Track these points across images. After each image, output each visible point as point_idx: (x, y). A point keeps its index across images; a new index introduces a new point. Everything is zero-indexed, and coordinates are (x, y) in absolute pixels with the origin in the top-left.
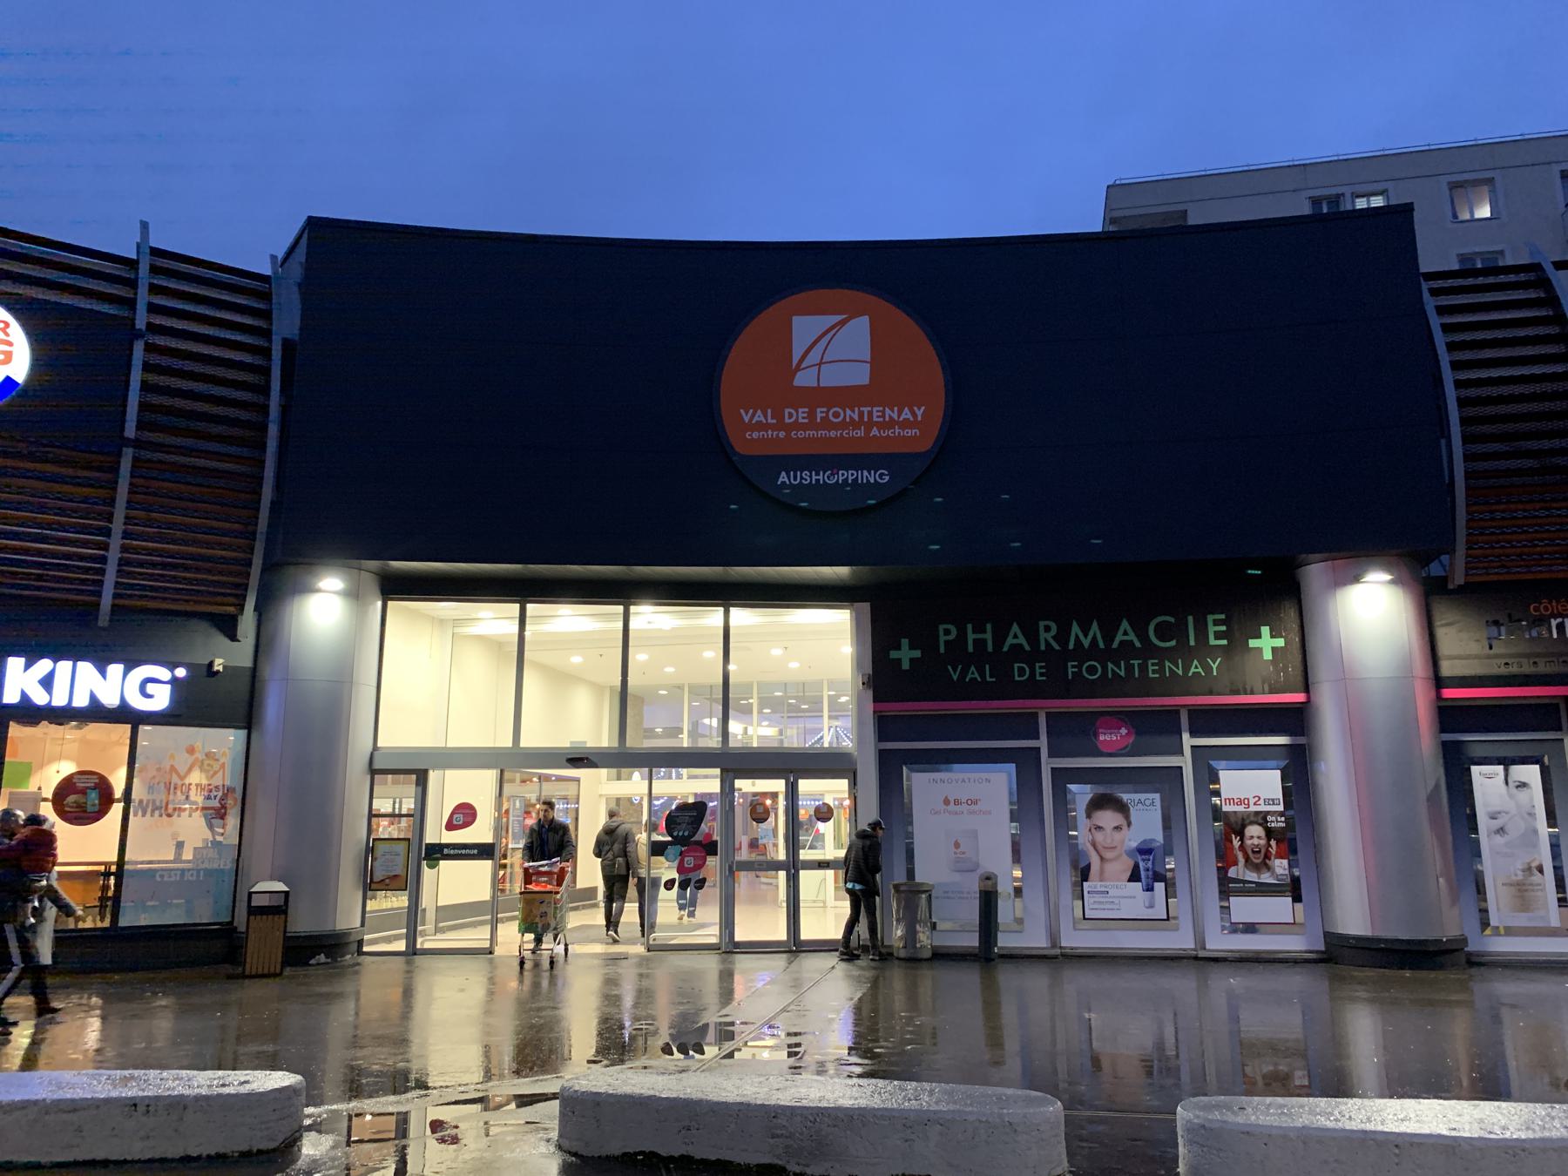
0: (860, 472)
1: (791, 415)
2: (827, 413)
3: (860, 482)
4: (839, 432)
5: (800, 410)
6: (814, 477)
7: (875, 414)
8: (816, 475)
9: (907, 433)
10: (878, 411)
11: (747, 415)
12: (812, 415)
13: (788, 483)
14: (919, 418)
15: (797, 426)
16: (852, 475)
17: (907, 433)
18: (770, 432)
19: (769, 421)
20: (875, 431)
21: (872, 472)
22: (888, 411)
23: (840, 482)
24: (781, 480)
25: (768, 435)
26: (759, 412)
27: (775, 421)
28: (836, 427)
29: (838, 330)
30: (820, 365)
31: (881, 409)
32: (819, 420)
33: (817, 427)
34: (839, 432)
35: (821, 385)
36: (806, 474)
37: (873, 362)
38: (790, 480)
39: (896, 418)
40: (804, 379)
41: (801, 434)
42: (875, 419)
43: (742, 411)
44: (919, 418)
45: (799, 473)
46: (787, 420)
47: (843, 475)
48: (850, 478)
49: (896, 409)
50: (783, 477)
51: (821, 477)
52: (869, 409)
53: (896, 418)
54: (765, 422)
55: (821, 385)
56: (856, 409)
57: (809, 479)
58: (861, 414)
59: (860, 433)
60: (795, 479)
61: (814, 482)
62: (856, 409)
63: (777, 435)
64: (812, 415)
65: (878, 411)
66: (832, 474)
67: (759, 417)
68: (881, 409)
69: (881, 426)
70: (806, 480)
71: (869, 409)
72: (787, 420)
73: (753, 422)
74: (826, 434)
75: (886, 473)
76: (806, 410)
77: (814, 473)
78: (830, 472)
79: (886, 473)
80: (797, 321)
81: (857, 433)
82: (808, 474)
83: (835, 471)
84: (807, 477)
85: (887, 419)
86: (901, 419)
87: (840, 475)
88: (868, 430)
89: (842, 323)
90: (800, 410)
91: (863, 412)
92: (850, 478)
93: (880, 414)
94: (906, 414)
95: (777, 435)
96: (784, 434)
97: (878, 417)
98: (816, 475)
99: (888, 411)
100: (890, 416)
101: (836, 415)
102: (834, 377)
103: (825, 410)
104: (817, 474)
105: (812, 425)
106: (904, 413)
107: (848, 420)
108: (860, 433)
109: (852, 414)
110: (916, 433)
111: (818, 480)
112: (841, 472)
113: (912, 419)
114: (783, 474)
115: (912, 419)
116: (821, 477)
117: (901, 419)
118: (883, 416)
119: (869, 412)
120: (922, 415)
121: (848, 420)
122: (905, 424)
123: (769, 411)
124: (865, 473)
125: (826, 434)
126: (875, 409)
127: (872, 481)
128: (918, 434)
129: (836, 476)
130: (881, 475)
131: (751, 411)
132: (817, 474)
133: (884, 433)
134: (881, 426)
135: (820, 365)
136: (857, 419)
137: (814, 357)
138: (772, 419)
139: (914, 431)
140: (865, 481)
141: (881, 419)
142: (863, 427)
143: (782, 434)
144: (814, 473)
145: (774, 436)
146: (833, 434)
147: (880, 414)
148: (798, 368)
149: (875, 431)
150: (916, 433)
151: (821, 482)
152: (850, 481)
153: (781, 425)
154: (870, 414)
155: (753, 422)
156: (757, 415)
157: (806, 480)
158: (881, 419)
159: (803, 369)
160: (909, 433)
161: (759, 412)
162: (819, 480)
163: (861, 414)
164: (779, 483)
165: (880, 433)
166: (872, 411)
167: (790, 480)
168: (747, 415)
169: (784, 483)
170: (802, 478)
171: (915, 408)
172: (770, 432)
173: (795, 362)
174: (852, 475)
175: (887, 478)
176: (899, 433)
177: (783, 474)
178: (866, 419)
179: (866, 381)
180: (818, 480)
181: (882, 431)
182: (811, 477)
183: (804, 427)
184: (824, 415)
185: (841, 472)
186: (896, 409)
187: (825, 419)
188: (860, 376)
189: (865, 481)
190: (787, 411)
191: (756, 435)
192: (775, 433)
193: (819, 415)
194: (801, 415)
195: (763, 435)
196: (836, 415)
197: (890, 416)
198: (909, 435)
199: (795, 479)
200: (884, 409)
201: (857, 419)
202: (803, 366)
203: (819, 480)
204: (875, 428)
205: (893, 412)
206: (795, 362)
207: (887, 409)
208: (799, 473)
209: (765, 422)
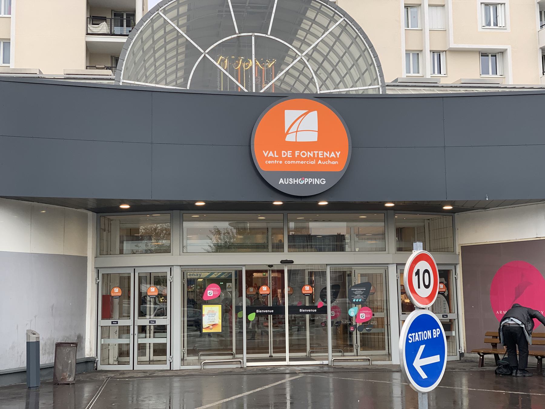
0: (313, 179)
1: (284, 154)
2: (300, 153)
3: (313, 183)
4: (305, 162)
5: (289, 152)
6: (294, 181)
7: (320, 154)
8: (295, 180)
9: (333, 163)
10: (321, 153)
11: (266, 153)
12: (293, 154)
13: (283, 183)
14: (338, 157)
15: (287, 158)
16: (310, 180)
17: (333, 163)
18: (276, 161)
19: (276, 156)
21: (319, 179)
23: (305, 183)
25: (275, 162)
26: (271, 152)
27: (278, 156)
28: (304, 159)
30: (297, 131)
31: (322, 152)
32: (296, 156)
33: (296, 159)
34: (305, 162)
35: (297, 141)
36: (291, 180)
38: (284, 182)
39: (328, 155)
40: (290, 138)
41: (289, 162)
42: (320, 157)
43: (264, 151)
44: (338, 157)
45: (288, 179)
46: (283, 156)
47: (306, 180)
48: (310, 182)
49: (328, 152)
50: (281, 181)
51: (297, 181)
52: (317, 152)
54: (273, 156)
55: (297, 141)
56: (312, 152)
57: (292, 182)
59: (313, 162)
60: (286, 182)
61: (294, 183)
62: (312, 152)
65: (321, 153)
66: (302, 180)
67: (271, 154)
68: (322, 152)
70: (291, 182)
71: (317, 152)
72: (283, 156)
73: (269, 156)
74: (299, 162)
76: (291, 152)
77: (294, 179)
78: (301, 179)
79: (325, 180)
80: (287, 113)
82: (292, 180)
84: (292, 181)
85: (325, 157)
87: (305, 180)
88: (317, 162)
89: (306, 114)
91: (315, 153)
92: (310, 182)
93: (322, 154)
95: (279, 162)
96: (282, 162)
97: (321, 155)
98: (295, 180)
99: (325, 153)
100: (326, 156)
101: (304, 154)
102: (303, 138)
103: (299, 152)
104: (296, 180)
105: (293, 158)
106: (332, 154)
107: (308, 156)
108: (313, 162)
110: (337, 163)
111: (296, 183)
112: (305, 179)
113: (335, 157)
114: (281, 179)
115: (335, 157)
116: (297, 181)
117: (331, 157)
118: (323, 155)
119: (317, 153)
120: (339, 155)
121: (308, 156)
122: (332, 159)
123: (275, 152)
124: (316, 179)
125: (299, 162)
126: (320, 152)
127: (319, 183)
128: (338, 163)
129: (304, 181)
130: (322, 181)
131: (268, 152)
132: (296, 180)
134: (323, 159)
135: (297, 131)
136: (312, 156)
137: (294, 129)
138: (276, 155)
139: (336, 162)
140: (316, 183)
141: (322, 157)
142: (315, 160)
143: (281, 162)
144: (294, 179)
145: (278, 163)
146: (302, 162)
147: (322, 154)
148: (287, 133)
149: (320, 162)
151: (297, 183)
152: (309, 183)
153: (280, 158)
154: (318, 154)
155: (269, 156)
156: (270, 154)
157: (291, 182)
158: (322, 157)
159: (290, 133)
160: (334, 163)
161: (271, 152)
162: (296, 182)
163: (314, 154)
164: (280, 183)
165: (322, 163)
166: (319, 153)
167: (284, 182)
168: (266, 153)
170: (289, 181)
171: (336, 152)
172: (276, 161)
173: (286, 131)
174: (310, 180)
175: (325, 182)
176: (330, 163)
177: (281, 179)
178: (316, 157)
179: (316, 139)
180: (296, 183)
181: (323, 162)
182: (293, 181)
184: (298, 154)
185: (305, 179)
186: (328, 152)
187: (299, 156)
188: (313, 137)
189: (316, 183)
190: (283, 152)
191: (269, 162)
192: (278, 162)
193: (296, 154)
194: (289, 154)
195: (273, 162)
196: (304, 154)
197: (326, 156)
198: (334, 163)
199: (286, 182)
200: (324, 152)
201: (312, 156)
202: (289, 133)
203: (296, 182)
204: (320, 161)
205: (327, 154)
206: (286, 131)
207: (325, 152)
208: (288, 179)
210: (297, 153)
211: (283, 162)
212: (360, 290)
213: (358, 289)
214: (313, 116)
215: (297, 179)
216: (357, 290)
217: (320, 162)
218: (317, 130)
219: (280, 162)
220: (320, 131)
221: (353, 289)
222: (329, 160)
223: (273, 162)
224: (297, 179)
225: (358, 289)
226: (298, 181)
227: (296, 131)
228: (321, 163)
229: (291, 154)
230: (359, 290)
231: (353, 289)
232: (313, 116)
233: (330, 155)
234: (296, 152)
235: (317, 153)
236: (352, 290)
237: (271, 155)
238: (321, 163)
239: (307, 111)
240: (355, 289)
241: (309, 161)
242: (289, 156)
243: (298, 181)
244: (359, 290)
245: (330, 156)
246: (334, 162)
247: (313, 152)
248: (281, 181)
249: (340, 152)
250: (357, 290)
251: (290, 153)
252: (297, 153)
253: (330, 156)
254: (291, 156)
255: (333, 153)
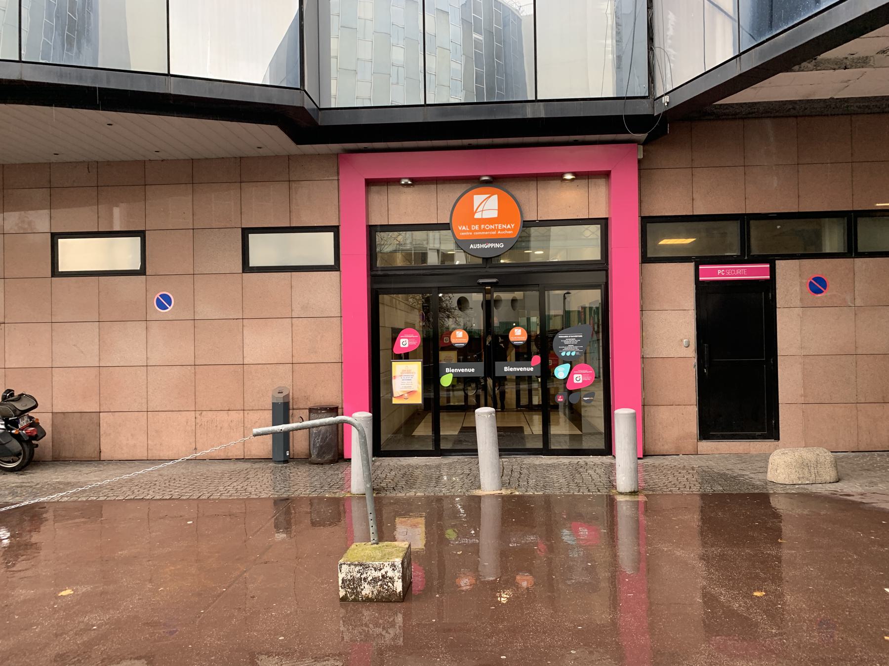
5: (477, 226)
6: (481, 246)
7: (499, 227)
12: (480, 227)
15: (475, 231)
19: (467, 229)
20: (499, 232)
26: (464, 227)
30: (482, 211)
37: (499, 210)
39: (505, 227)
40: (477, 216)
41: (477, 233)
42: (499, 228)
50: (472, 246)
58: (495, 226)
59: (494, 233)
67: (464, 228)
69: (501, 230)
72: (473, 229)
84: (479, 246)
88: (497, 232)
89: (489, 197)
99: (503, 226)
101: (487, 227)
102: (487, 215)
105: (480, 230)
108: (494, 233)
114: (472, 245)
116: (483, 246)
122: (508, 230)
126: (499, 225)
127: (498, 247)
134: (501, 230)
135: (482, 211)
137: (480, 209)
143: (471, 234)
146: (486, 233)
148: (476, 212)
153: (470, 231)
154: (498, 227)
160: (510, 232)
161: (464, 227)
163: (495, 226)
173: (475, 210)
177: (472, 245)
179: (496, 216)
187: (484, 228)
188: (494, 214)
190: (472, 226)
191: (463, 234)
196: (487, 227)
206: (475, 210)
210: (482, 226)
211: (473, 234)
212: (572, 338)
213: (570, 336)
214: (495, 198)
216: (568, 338)
217: (499, 232)
220: (499, 210)
221: (562, 337)
225: (570, 336)
226: (483, 246)
230: (571, 338)
231: (562, 337)
232: (495, 198)
233: (507, 227)
236: (559, 337)
240: (565, 337)
243: (483, 246)
244: (571, 338)
250: (568, 338)
253: (507, 227)
255: (509, 225)
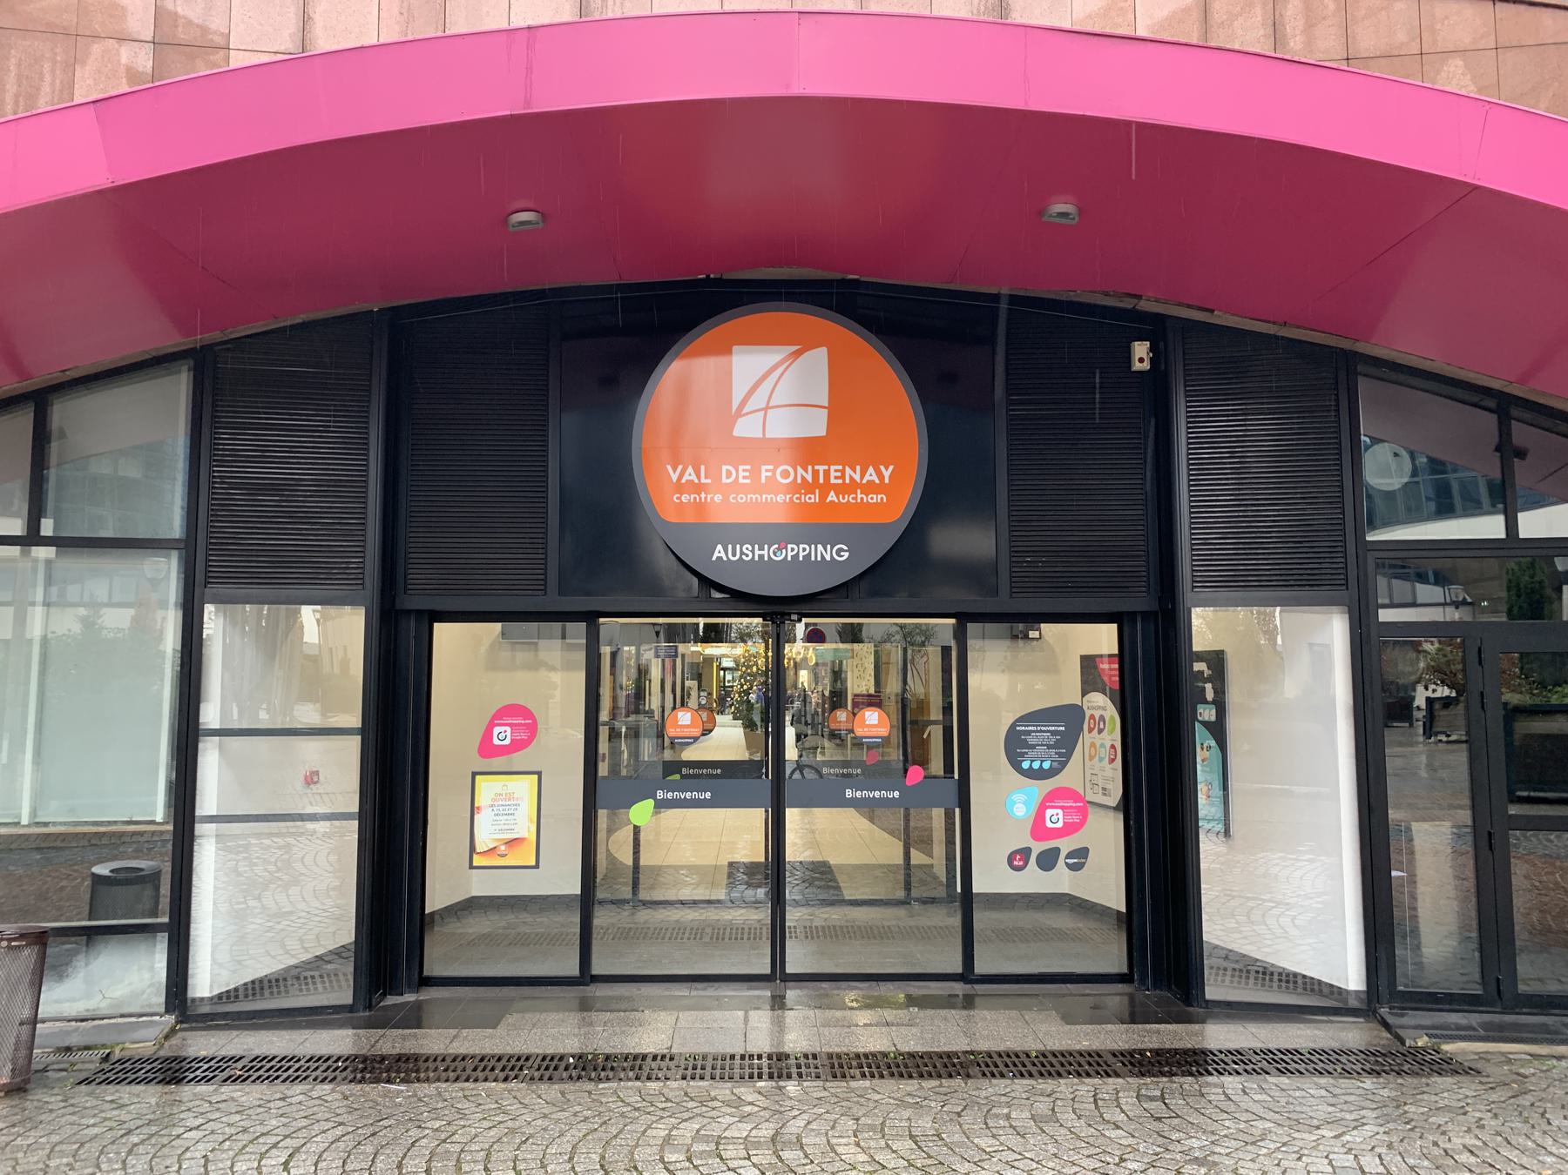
0: (813, 546)
1: (729, 474)
2: (774, 471)
3: (813, 559)
4: (788, 497)
5: (741, 468)
6: (757, 552)
7: (833, 474)
10: (836, 471)
11: (674, 472)
12: (755, 474)
13: (725, 559)
14: (887, 481)
15: (736, 487)
16: (804, 550)
18: (703, 495)
19: (703, 480)
21: (829, 546)
22: (848, 471)
23: (789, 559)
24: (716, 555)
25: (700, 499)
26: (690, 470)
29: (788, 367)
30: (766, 409)
31: (840, 467)
32: (763, 480)
39: (858, 481)
41: (742, 498)
42: (833, 481)
43: (669, 467)
44: (887, 481)
45: (738, 546)
46: (725, 480)
47: (793, 550)
48: (802, 554)
49: (858, 468)
50: (719, 552)
51: (765, 553)
52: (826, 467)
53: (858, 481)
54: (696, 481)
55: (767, 436)
56: (810, 468)
59: (813, 498)
60: (734, 555)
61: (756, 559)
62: (810, 468)
63: (712, 498)
64: (755, 474)
65: (836, 471)
66: (778, 549)
69: (840, 490)
70: (747, 556)
71: (826, 467)
72: (725, 480)
73: (683, 481)
75: (846, 548)
76: (748, 467)
77: (756, 546)
78: (776, 546)
79: (846, 548)
81: (810, 498)
82: (750, 548)
83: (783, 544)
84: (749, 552)
85: (847, 481)
86: (864, 481)
88: (824, 496)
90: (741, 468)
92: (802, 554)
93: (839, 474)
94: (871, 475)
95: (712, 498)
96: (721, 497)
97: (836, 478)
99: (848, 471)
103: (771, 467)
104: (761, 549)
105: (756, 487)
106: (868, 473)
109: (804, 474)
110: (882, 498)
111: (761, 557)
112: (790, 546)
113: (877, 481)
114: (719, 547)
115: (877, 481)
116: (765, 553)
117: (864, 481)
118: (843, 477)
119: (824, 471)
120: (890, 477)
121: (799, 481)
122: (869, 488)
124: (820, 547)
127: (828, 558)
129: (784, 551)
130: (839, 552)
131: (680, 467)
132: (761, 549)
133: (844, 498)
134: (840, 490)
135: (766, 409)
136: (810, 480)
137: (758, 400)
138: (706, 478)
139: (879, 496)
140: (819, 559)
141: (840, 481)
142: (817, 491)
144: (756, 546)
147: (839, 474)
148: (739, 414)
149: (832, 497)
150: (882, 498)
151: (766, 559)
152: (801, 559)
154: (827, 473)
157: (747, 556)
158: (840, 481)
159: (747, 414)
160: (874, 498)
161: (690, 470)
163: (815, 473)
164: (714, 559)
165: (838, 498)
166: (829, 470)
168: (674, 472)
169: (719, 558)
170: (742, 553)
171: (882, 468)
173: (734, 409)
174: (804, 550)
175: (846, 555)
176: (862, 499)
177: (719, 547)
178: (821, 481)
180: (761, 557)
182: (753, 551)
183: (744, 489)
184: (769, 474)
185: (790, 546)
186: (858, 468)
189: (819, 559)
190: (724, 468)
193: (764, 474)
194: (742, 474)
195: (695, 498)
197: (851, 478)
199: (734, 555)
201: (810, 480)
202: (744, 411)
204: (832, 493)
206: (734, 409)
208: (738, 546)
209: (696, 481)
215: (766, 546)
217: (832, 497)
218: (827, 405)
219: (716, 499)
222: (859, 491)
223: (695, 498)
224: (766, 546)
227: (764, 406)
228: (835, 499)
229: (747, 474)
233: (862, 476)
234: (764, 468)
235: (824, 471)
237: (690, 478)
238: (835, 499)
239: (799, 347)
241: (801, 494)
242: (741, 481)
245: (862, 479)
246: (875, 496)
247: (813, 470)
248: (719, 552)
249: (891, 468)
251: (744, 470)
252: (767, 471)
253: (862, 479)
254: (748, 481)
255: (871, 470)
